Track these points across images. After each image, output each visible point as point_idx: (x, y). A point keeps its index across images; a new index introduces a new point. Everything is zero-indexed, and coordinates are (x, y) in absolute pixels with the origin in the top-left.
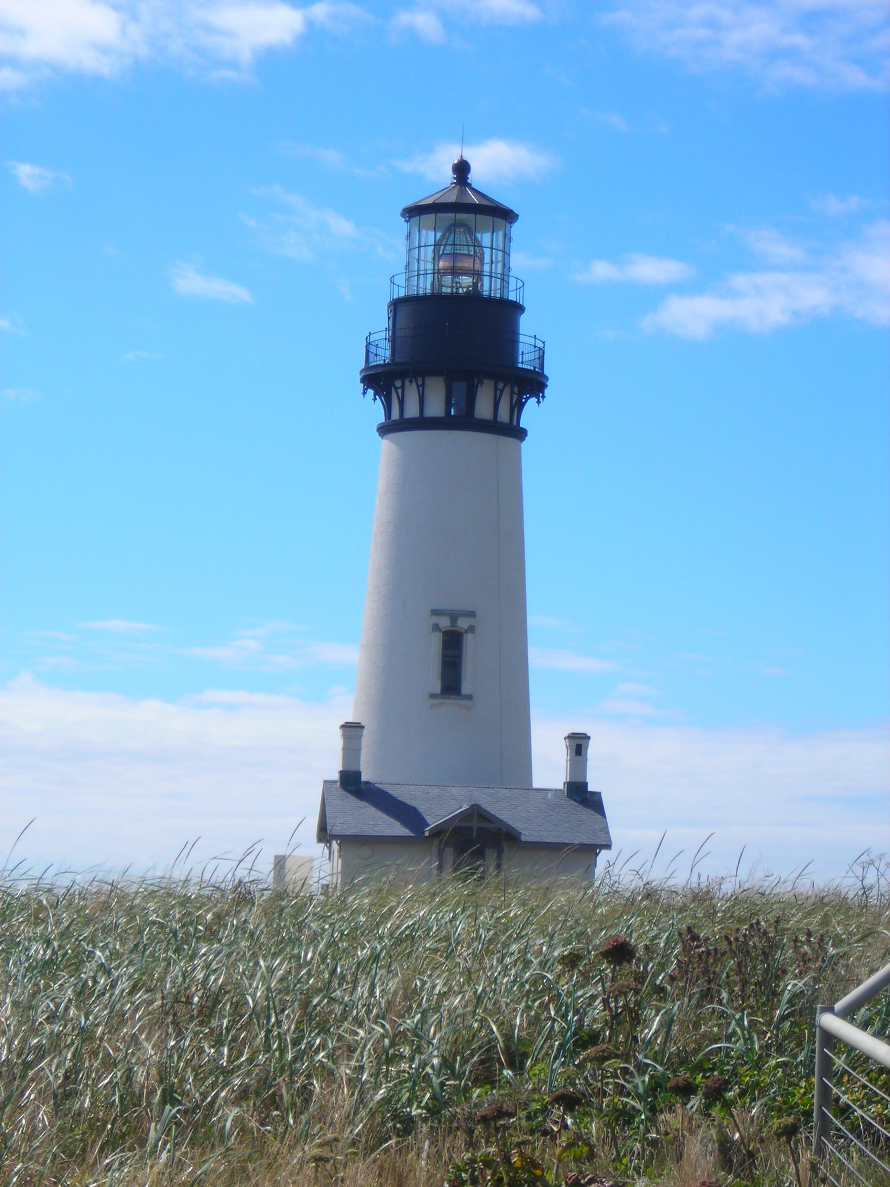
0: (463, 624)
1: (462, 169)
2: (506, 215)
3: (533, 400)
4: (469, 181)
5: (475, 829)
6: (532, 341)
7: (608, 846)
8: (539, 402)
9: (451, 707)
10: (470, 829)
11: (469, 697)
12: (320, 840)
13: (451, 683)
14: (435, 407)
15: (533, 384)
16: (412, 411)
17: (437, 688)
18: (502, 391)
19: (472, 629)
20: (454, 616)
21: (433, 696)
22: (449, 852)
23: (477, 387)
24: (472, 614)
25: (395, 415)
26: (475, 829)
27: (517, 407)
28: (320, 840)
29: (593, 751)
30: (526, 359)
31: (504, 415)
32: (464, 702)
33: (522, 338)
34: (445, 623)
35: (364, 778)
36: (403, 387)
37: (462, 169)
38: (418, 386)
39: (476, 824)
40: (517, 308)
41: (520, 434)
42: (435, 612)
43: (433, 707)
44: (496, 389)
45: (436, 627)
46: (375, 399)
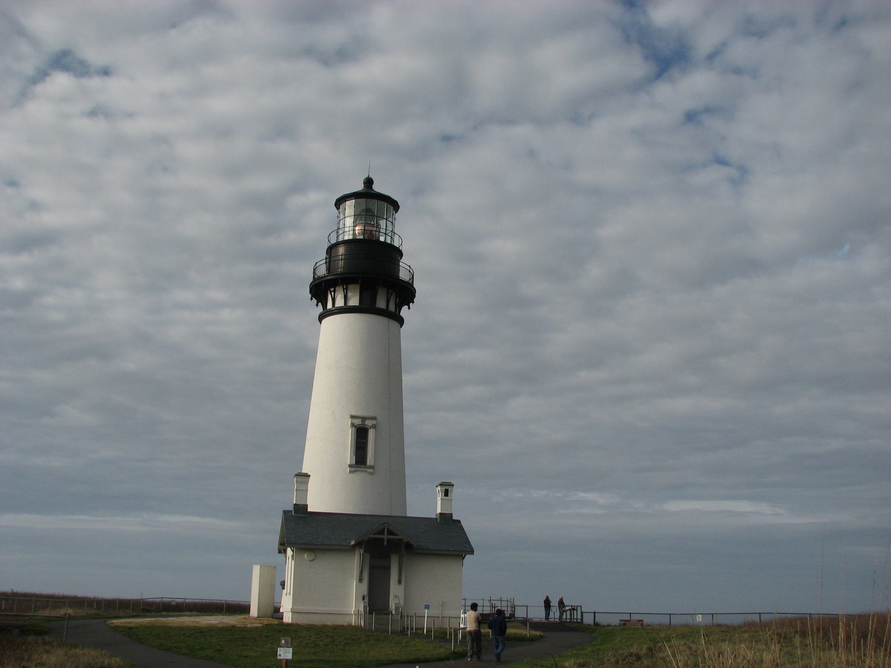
0: (369, 423)
1: (369, 182)
3: (406, 307)
7: (471, 552)
10: (383, 540)
11: (372, 467)
12: (280, 552)
14: (354, 301)
16: (340, 303)
19: (374, 427)
20: (364, 419)
21: (350, 466)
22: (368, 556)
24: (374, 418)
25: (330, 306)
27: (399, 307)
28: (280, 552)
29: (455, 492)
31: (392, 308)
32: (369, 470)
34: (358, 422)
35: (310, 509)
37: (369, 182)
41: (401, 321)
42: (352, 417)
45: (353, 425)
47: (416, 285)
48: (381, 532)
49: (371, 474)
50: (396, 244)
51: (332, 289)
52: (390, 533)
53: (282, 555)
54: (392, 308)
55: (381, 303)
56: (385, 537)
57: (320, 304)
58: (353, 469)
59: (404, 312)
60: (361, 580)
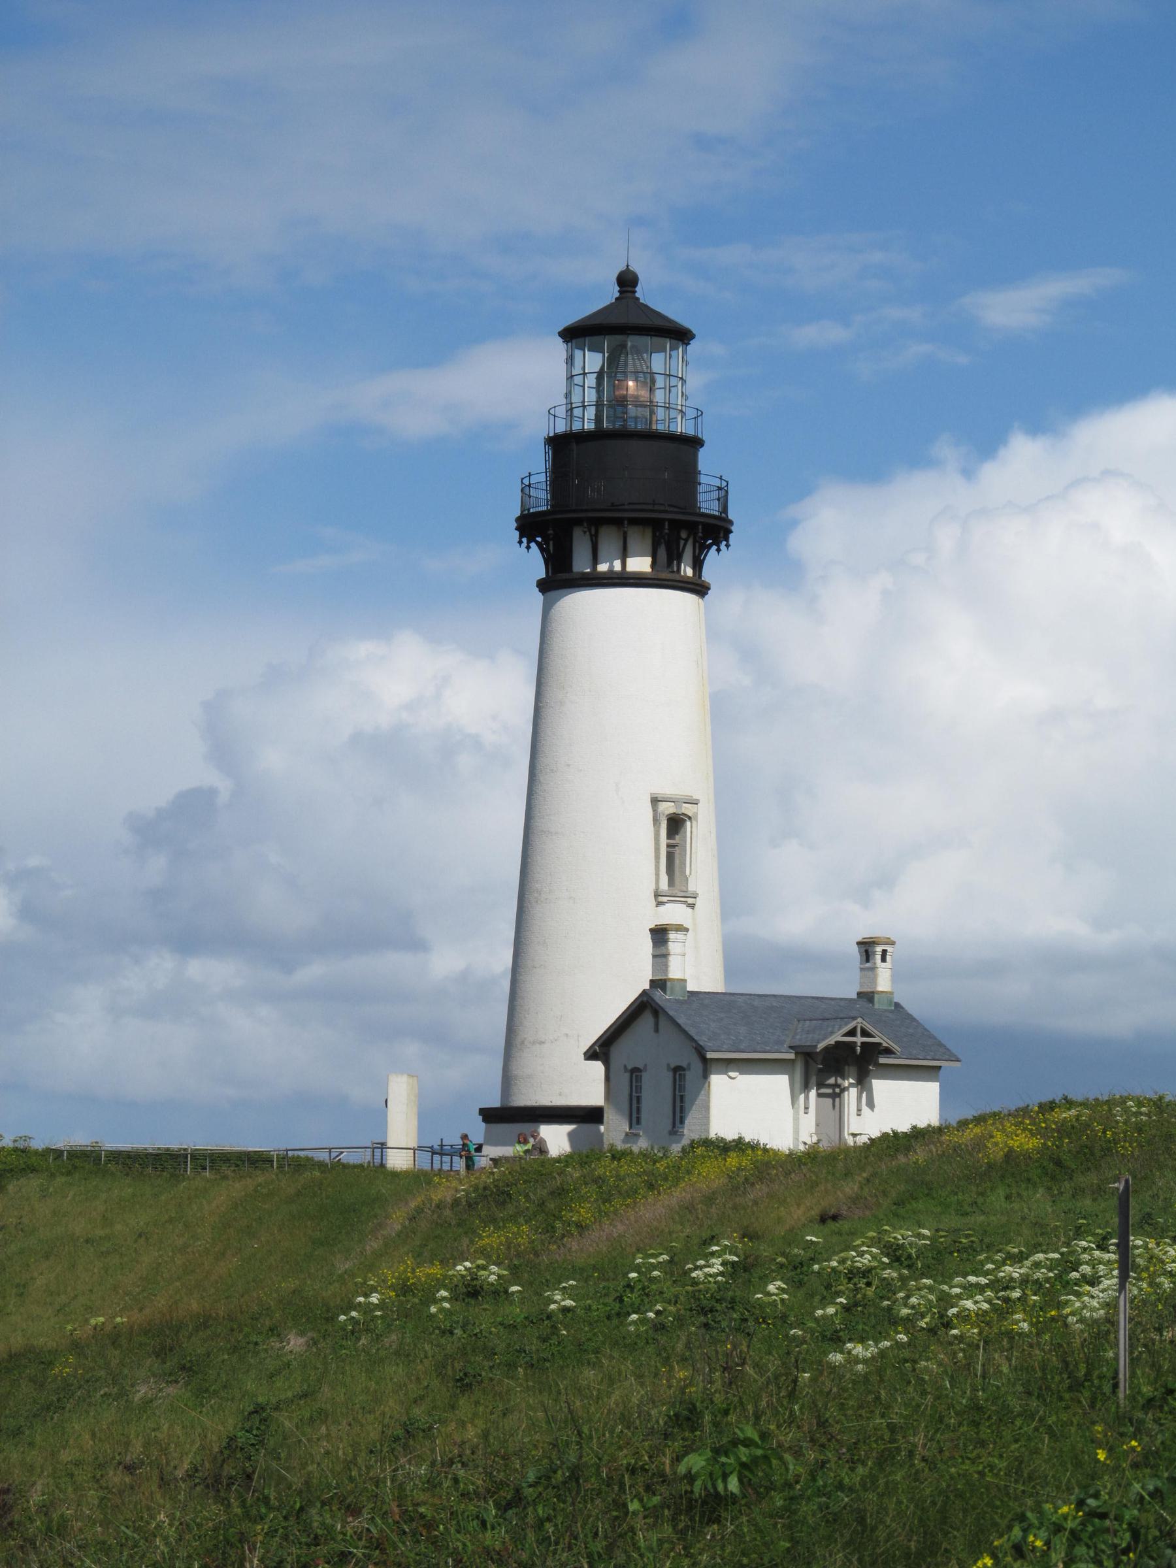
0: (687, 809)
1: (627, 281)
2: (681, 335)
4: (637, 295)
6: (717, 483)
12: (591, 1055)
14: (640, 564)
15: (716, 531)
17: (664, 885)
23: (686, 540)
25: (581, 565)
30: (708, 504)
32: (690, 901)
33: (703, 479)
34: (667, 808)
37: (627, 281)
38: (591, 535)
39: (859, 1039)
40: (695, 443)
43: (659, 904)
47: (730, 517)
48: (852, 1033)
49: (692, 906)
50: (690, 431)
52: (865, 1033)
53: (598, 1067)
56: (859, 1039)
57: (533, 545)
58: (665, 899)
60: (806, 1108)
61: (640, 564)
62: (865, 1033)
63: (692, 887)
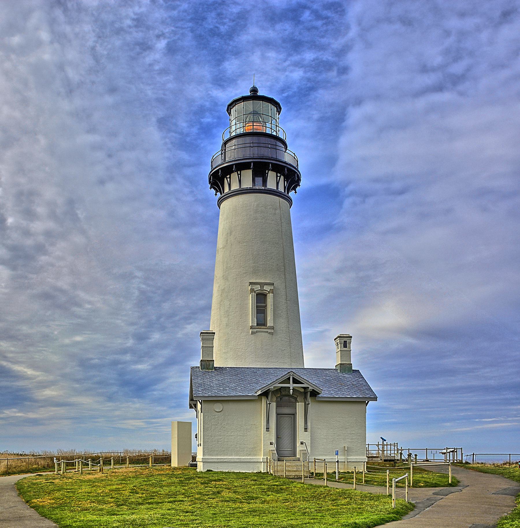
1: (254, 90)
5: (291, 388)
8: (296, 192)
9: (263, 335)
12: (191, 407)
13: (261, 323)
14: (247, 183)
16: (235, 187)
18: (280, 177)
20: (262, 284)
26: (291, 388)
28: (191, 407)
32: (269, 331)
34: (257, 288)
36: (230, 178)
44: (277, 176)
46: (216, 195)
48: (287, 381)
51: (228, 176)
52: (295, 381)
54: (281, 189)
55: (271, 184)
58: (255, 330)
59: (291, 194)
60: (268, 429)
61: (247, 183)
62: (295, 381)
63: (270, 323)
